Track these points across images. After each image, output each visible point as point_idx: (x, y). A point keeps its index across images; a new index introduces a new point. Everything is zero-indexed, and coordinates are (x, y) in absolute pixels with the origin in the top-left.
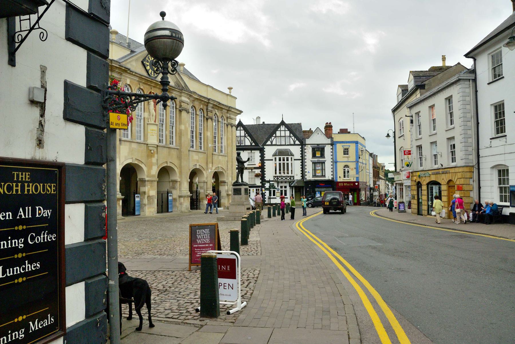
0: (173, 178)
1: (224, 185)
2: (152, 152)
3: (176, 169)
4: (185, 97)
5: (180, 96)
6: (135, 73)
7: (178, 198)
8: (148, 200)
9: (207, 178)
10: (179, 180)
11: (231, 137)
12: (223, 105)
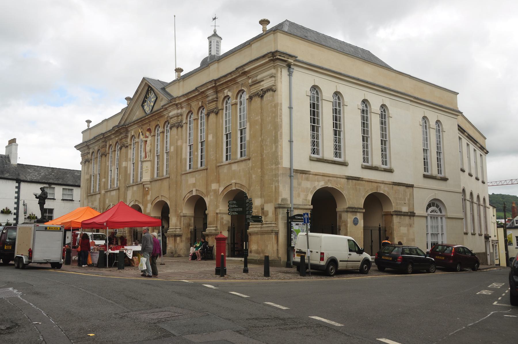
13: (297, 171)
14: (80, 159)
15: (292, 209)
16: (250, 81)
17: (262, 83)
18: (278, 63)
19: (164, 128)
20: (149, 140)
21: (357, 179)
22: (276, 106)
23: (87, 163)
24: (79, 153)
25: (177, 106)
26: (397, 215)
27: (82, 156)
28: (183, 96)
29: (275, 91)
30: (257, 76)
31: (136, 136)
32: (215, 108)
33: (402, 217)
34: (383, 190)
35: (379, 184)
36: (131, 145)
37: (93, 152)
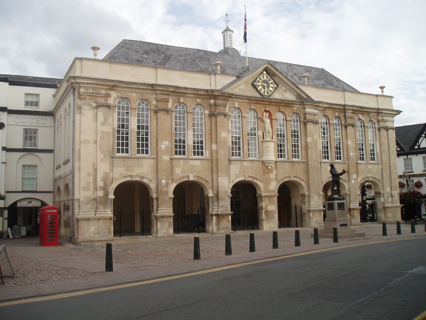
0: (301, 192)
1: (380, 197)
2: (269, 168)
3: (303, 183)
4: (311, 108)
5: (305, 108)
6: (242, 96)
7: (307, 213)
8: (266, 215)
9: (349, 190)
10: (307, 193)
11: (386, 142)
12: (368, 108)
17: (387, 123)
28: (328, 104)
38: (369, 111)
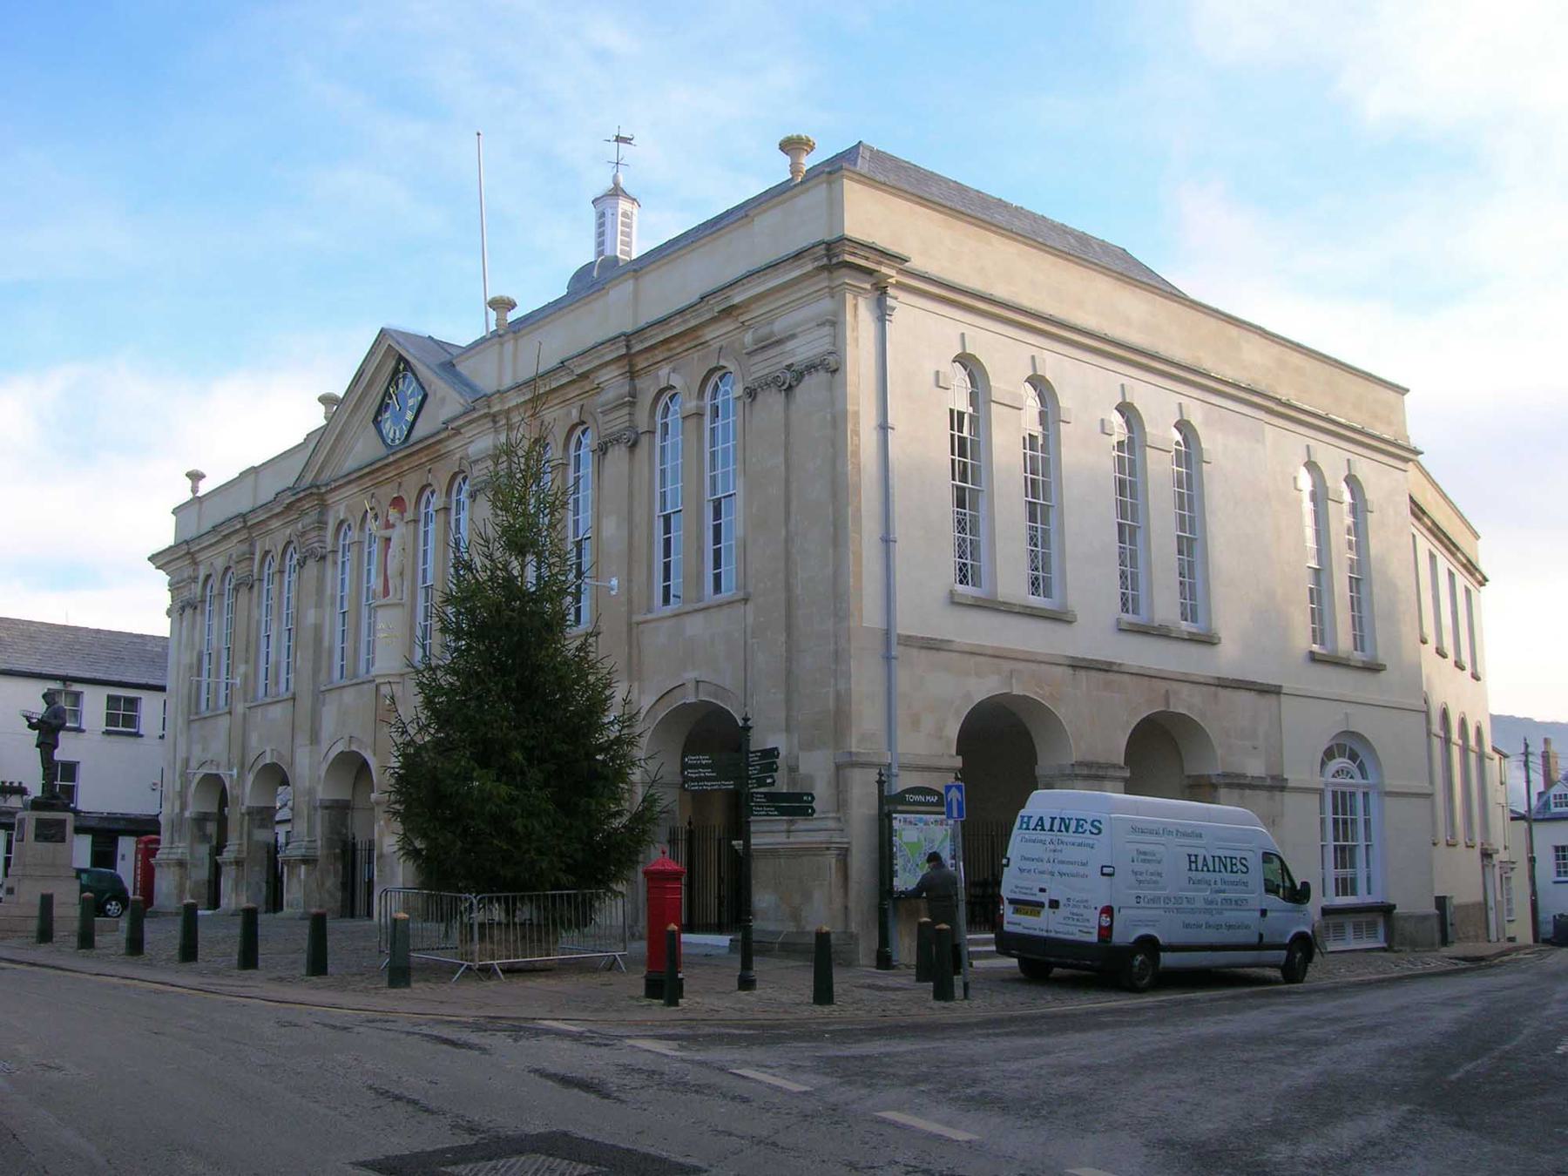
13: (908, 641)
14: (166, 599)
15: (894, 771)
16: (748, 338)
17: (790, 345)
18: (849, 279)
19: (449, 493)
20: (396, 535)
21: (1106, 668)
22: (837, 421)
23: (189, 611)
24: (163, 578)
25: (495, 422)
26: (1229, 786)
27: (173, 587)
28: (518, 387)
29: (835, 371)
30: (771, 323)
31: (355, 522)
32: (626, 429)
33: (1248, 792)
34: (1186, 703)
35: (1175, 685)
36: (335, 552)
37: (208, 577)
38: (676, 331)
